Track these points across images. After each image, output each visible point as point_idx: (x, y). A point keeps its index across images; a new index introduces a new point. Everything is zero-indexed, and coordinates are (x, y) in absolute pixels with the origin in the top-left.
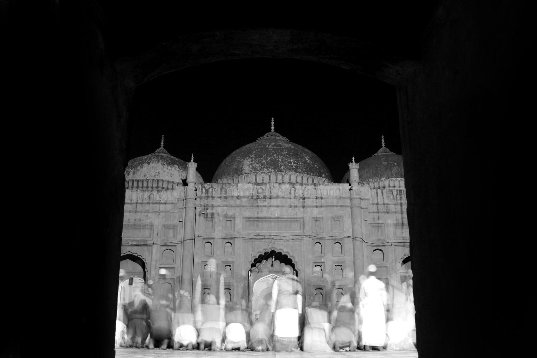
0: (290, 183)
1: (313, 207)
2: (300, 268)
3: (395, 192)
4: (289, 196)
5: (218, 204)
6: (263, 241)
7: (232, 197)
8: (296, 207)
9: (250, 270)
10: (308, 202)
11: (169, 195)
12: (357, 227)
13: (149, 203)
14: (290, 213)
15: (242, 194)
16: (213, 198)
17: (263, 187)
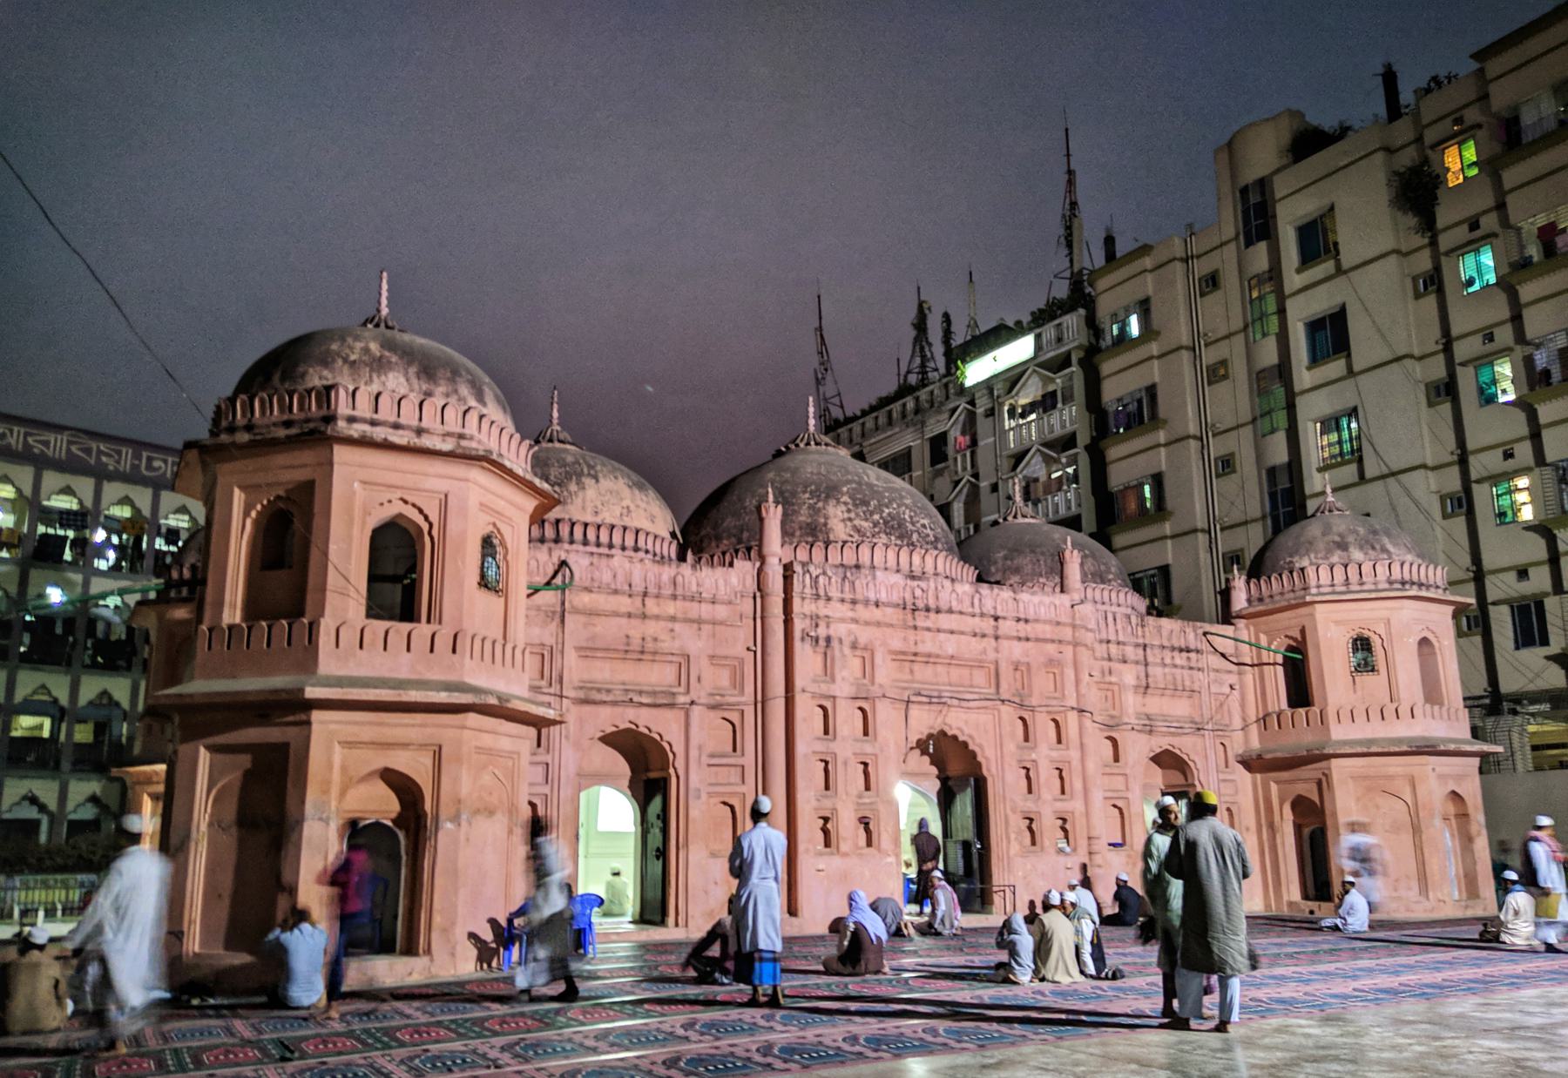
5: (838, 615)
7: (867, 602)
8: (984, 636)
10: (1007, 627)
11: (721, 582)
13: (674, 597)
15: (883, 597)
16: (829, 599)
17: (923, 584)
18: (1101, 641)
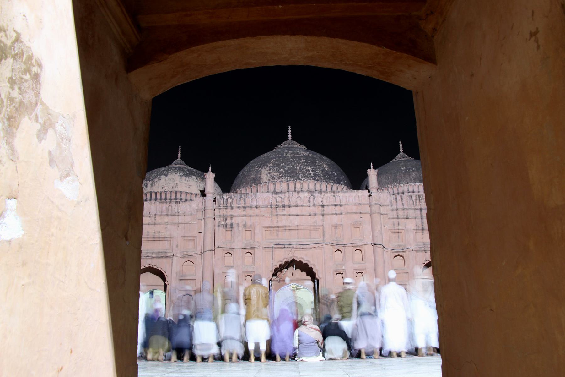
0: (308, 191)
1: (332, 214)
2: (321, 276)
3: (414, 198)
4: (308, 204)
5: (237, 214)
6: (283, 250)
7: (251, 207)
9: (271, 280)
11: (188, 207)
12: (377, 234)
13: (167, 215)
14: (310, 221)
15: (260, 203)
16: (232, 208)
17: (282, 196)
18: (392, 210)
